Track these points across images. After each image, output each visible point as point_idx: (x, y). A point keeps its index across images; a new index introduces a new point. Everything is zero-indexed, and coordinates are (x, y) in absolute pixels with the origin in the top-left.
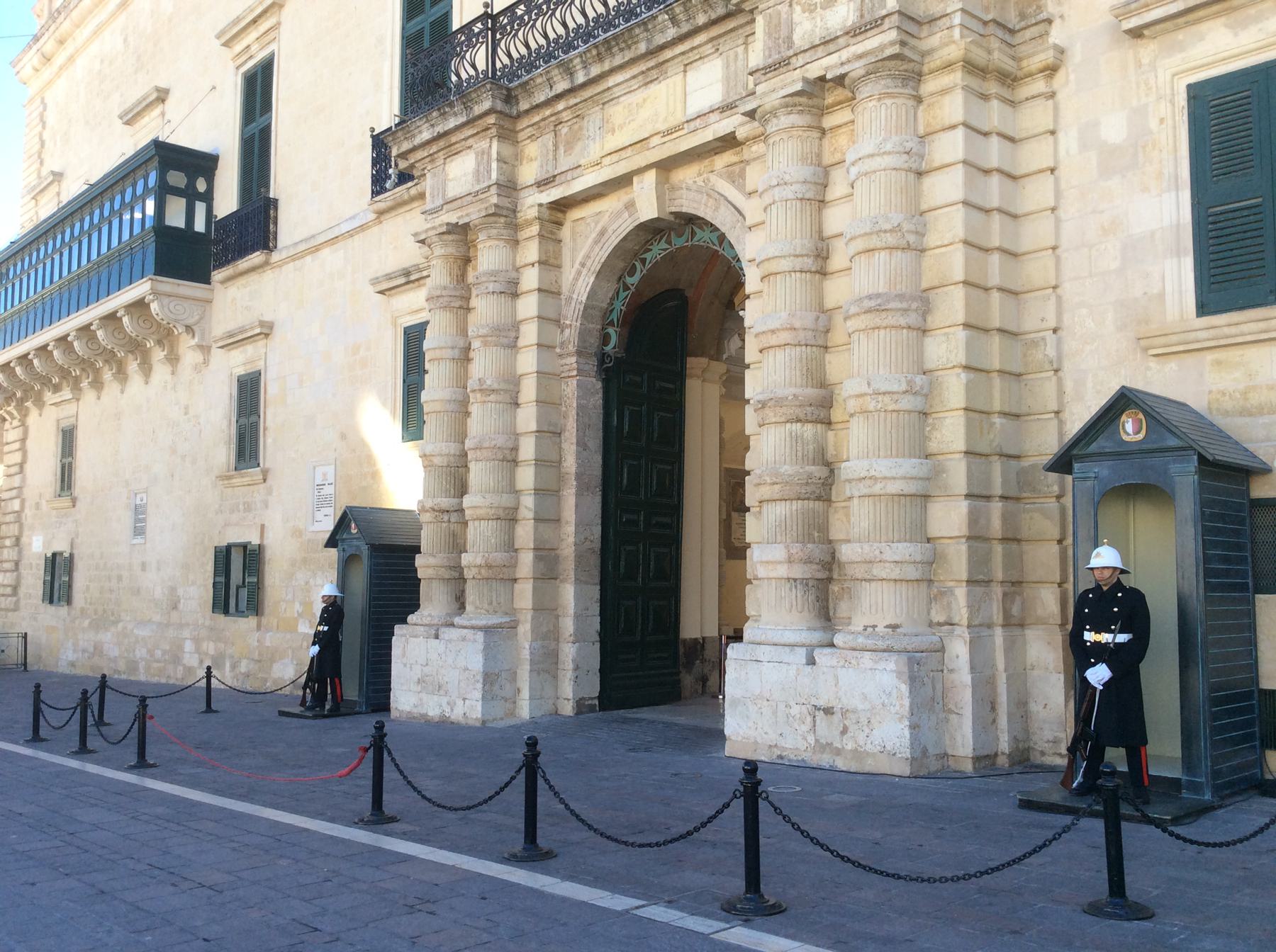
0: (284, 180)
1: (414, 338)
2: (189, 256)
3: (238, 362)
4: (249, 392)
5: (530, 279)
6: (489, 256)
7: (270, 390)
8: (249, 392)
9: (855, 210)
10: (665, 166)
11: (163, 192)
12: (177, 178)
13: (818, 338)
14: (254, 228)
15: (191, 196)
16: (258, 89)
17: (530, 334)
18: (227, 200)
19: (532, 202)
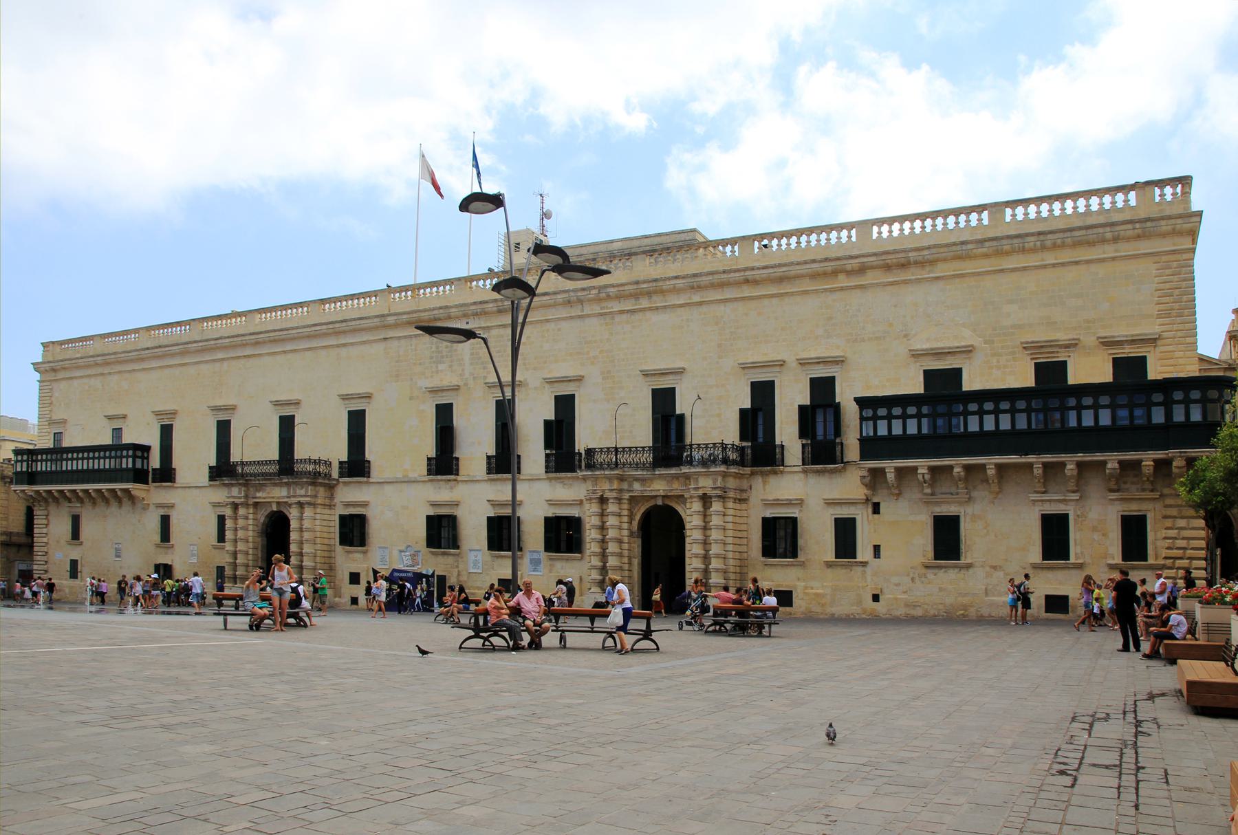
0: (176, 462)
1: (221, 520)
2: (140, 476)
3: (162, 512)
4: (165, 521)
5: (251, 516)
6: (242, 511)
7: (174, 522)
8: (165, 521)
9: (307, 524)
10: (278, 503)
11: (135, 457)
12: (139, 453)
13: (301, 543)
14: (166, 474)
15: (143, 458)
16: (167, 432)
17: (251, 528)
18: (155, 461)
19: (251, 501)
